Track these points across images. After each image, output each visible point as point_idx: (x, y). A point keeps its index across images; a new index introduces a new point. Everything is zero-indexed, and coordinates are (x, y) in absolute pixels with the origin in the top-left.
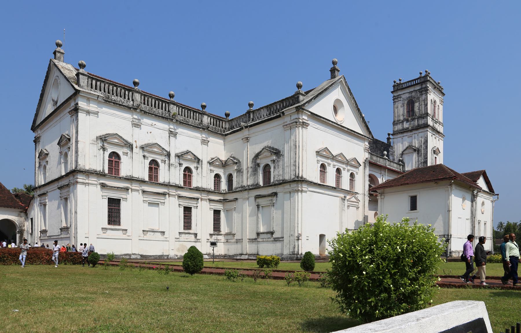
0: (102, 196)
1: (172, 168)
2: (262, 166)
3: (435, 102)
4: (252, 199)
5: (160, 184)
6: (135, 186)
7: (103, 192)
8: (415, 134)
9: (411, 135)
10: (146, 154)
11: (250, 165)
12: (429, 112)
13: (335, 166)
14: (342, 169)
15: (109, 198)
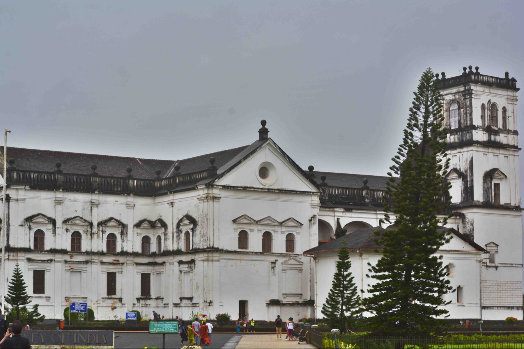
0: (28, 269)
1: (95, 236)
2: (184, 232)
3: (493, 107)
4: (176, 264)
5: (82, 253)
6: (58, 257)
7: (29, 266)
8: (459, 152)
9: (455, 153)
10: (69, 227)
11: (175, 230)
12: (474, 123)
13: (261, 230)
14: (272, 232)
15: (34, 270)
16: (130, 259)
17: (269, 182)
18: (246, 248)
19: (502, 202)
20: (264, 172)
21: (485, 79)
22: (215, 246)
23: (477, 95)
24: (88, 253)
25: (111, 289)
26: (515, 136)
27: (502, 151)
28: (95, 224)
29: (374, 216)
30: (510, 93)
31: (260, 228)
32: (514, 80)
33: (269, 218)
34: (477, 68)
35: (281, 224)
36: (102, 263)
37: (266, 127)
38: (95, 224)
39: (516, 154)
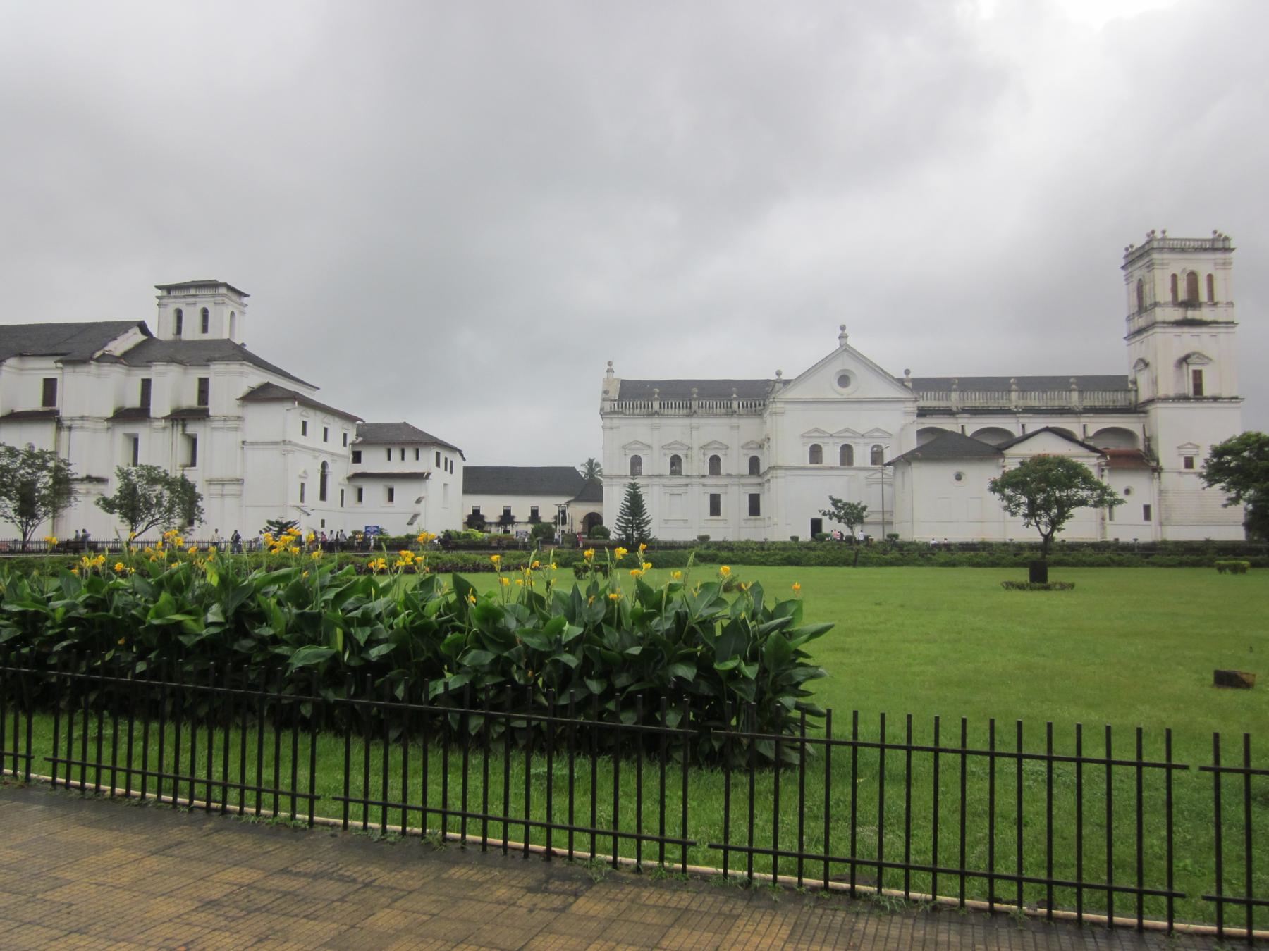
6: (656, 481)
16: (736, 481)
17: (846, 392)
18: (821, 463)
19: (1207, 391)
20: (844, 380)
21: (1177, 244)
22: (780, 463)
23: (1162, 264)
24: (687, 476)
25: (715, 509)
26: (1229, 309)
27: (1204, 330)
28: (696, 447)
29: (1014, 420)
30: (1219, 256)
31: (837, 440)
32: (1226, 239)
33: (847, 430)
34: (1164, 232)
35: (863, 436)
36: (704, 485)
37: (846, 332)
38: (696, 447)
39: (1230, 330)
